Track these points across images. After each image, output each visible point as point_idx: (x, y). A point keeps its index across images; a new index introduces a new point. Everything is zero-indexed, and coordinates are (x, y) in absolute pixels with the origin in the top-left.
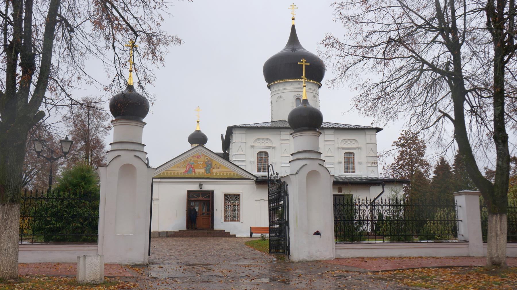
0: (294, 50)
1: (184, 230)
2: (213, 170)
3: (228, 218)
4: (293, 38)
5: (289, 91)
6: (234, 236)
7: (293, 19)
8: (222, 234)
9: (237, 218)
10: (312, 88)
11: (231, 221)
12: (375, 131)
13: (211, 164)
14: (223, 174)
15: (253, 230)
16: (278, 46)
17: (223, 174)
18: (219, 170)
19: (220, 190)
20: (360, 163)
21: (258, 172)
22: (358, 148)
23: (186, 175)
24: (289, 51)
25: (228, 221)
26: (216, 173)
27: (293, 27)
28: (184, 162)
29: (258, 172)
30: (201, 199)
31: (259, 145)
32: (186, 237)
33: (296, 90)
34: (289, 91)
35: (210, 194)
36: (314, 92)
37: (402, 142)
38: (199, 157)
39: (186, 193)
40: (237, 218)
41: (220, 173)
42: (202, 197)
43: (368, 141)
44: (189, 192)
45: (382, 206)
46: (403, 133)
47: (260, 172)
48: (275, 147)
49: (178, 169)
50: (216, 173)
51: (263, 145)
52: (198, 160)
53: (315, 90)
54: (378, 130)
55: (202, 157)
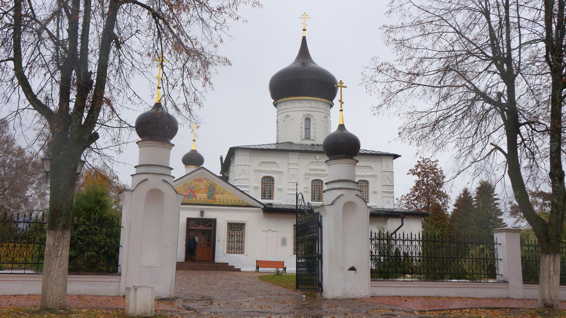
0: (303, 64)
1: (183, 263)
2: (216, 195)
3: (230, 250)
4: (304, 51)
5: (298, 109)
6: (239, 270)
7: (304, 30)
8: (225, 267)
9: (241, 250)
10: (323, 107)
11: (234, 253)
12: (393, 157)
13: (214, 189)
14: (227, 200)
15: (259, 264)
16: (287, 59)
17: (227, 200)
18: (222, 196)
19: (223, 218)
20: (375, 193)
21: (262, 199)
22: (374, 176)
24: (298, 65)
25: (231, 253)
26: (220, 200)
27: (304, 38)
28: (185, 186)
29: (262, 199)
30: (201, 227)
31: (264, 169)
32: (185, 269)
33: (305, 109)
34: (298, 109)
35: (212, 223)
36: (325, 112)
37: (419, 170)
38: (200, 180)
39: (186, 220)
40: (241, 250)
41: (224, 200)
42: (203, 225)
43: (384, 169)
44: (189, 220)
45: (411, 241)
46: (420, 160)
47: (265, 199)
48: (282, 172)
50: (220, 200)
51: (268, 169)
52: (200, 184)
53: (326, 110)
54: (396, 156)
55: (204, 181)
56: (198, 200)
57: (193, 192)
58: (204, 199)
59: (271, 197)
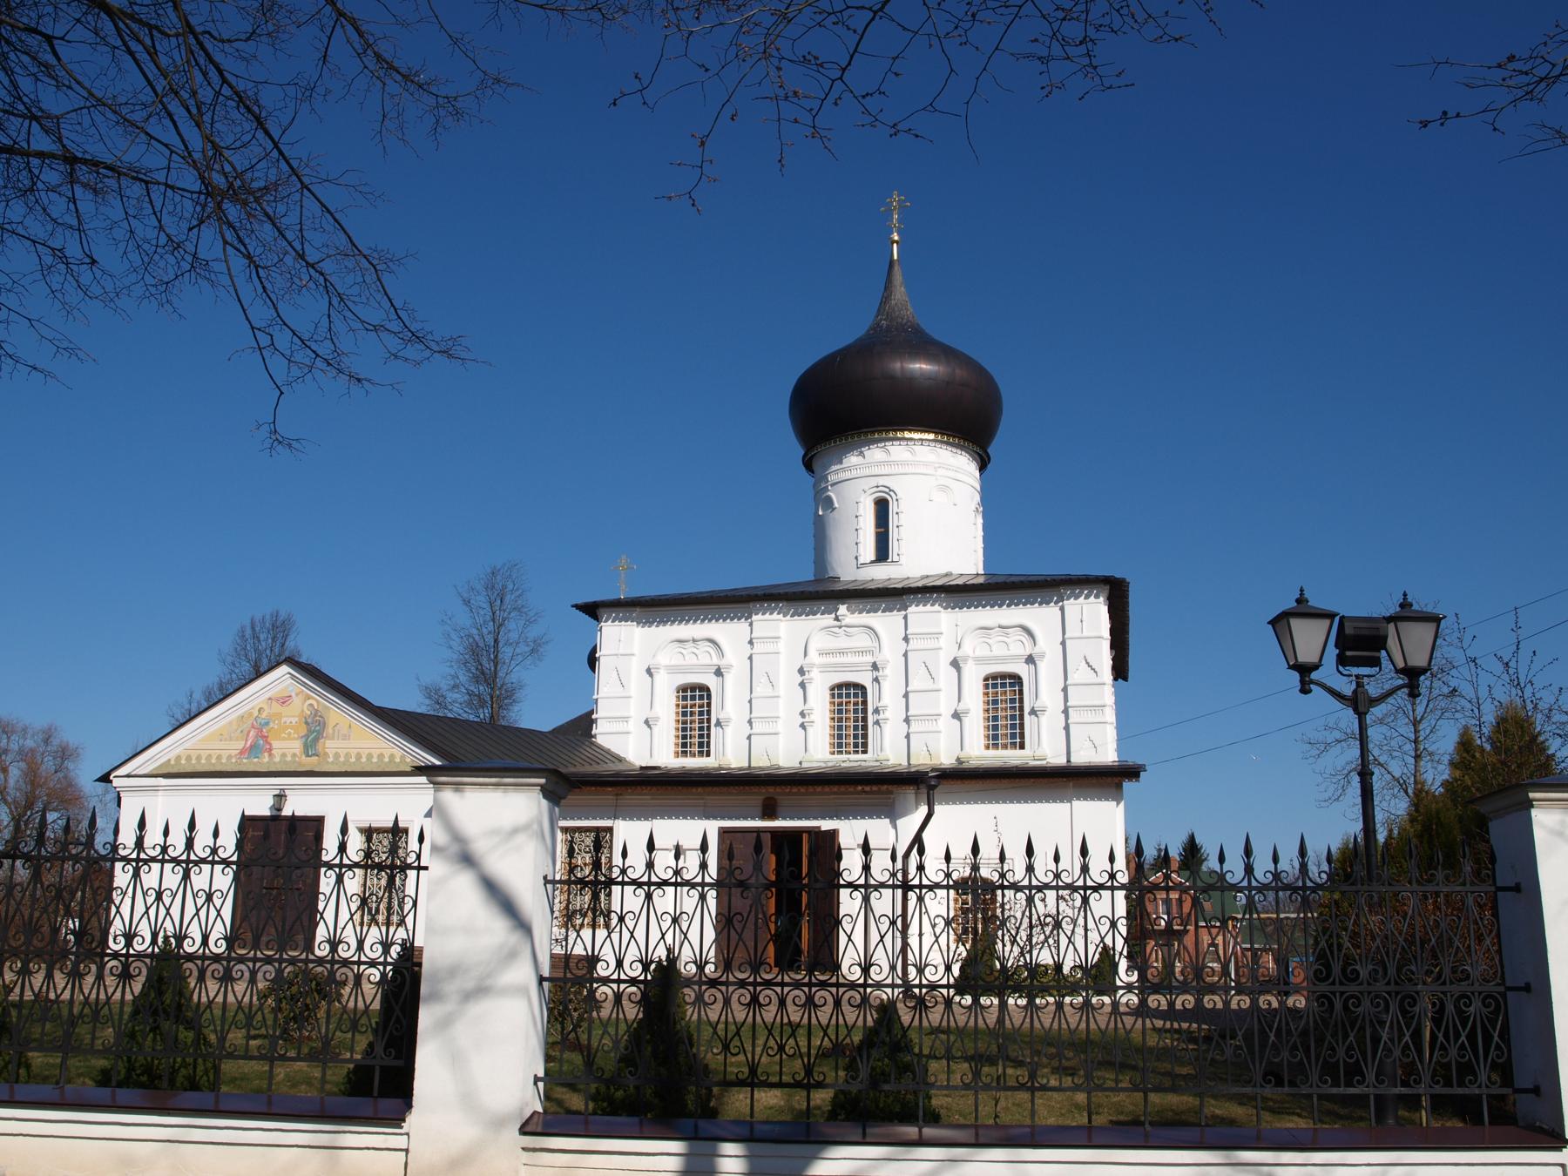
2: (328, 743)
13: (323, 724)
17: (359, 756)
23: (248, 764)
26: (337, 755)
49: (223, 745)
50: (337, 755)
56: (277, 759)
57: (265, 738)
58: (294, 755)
59: (704, 749)
